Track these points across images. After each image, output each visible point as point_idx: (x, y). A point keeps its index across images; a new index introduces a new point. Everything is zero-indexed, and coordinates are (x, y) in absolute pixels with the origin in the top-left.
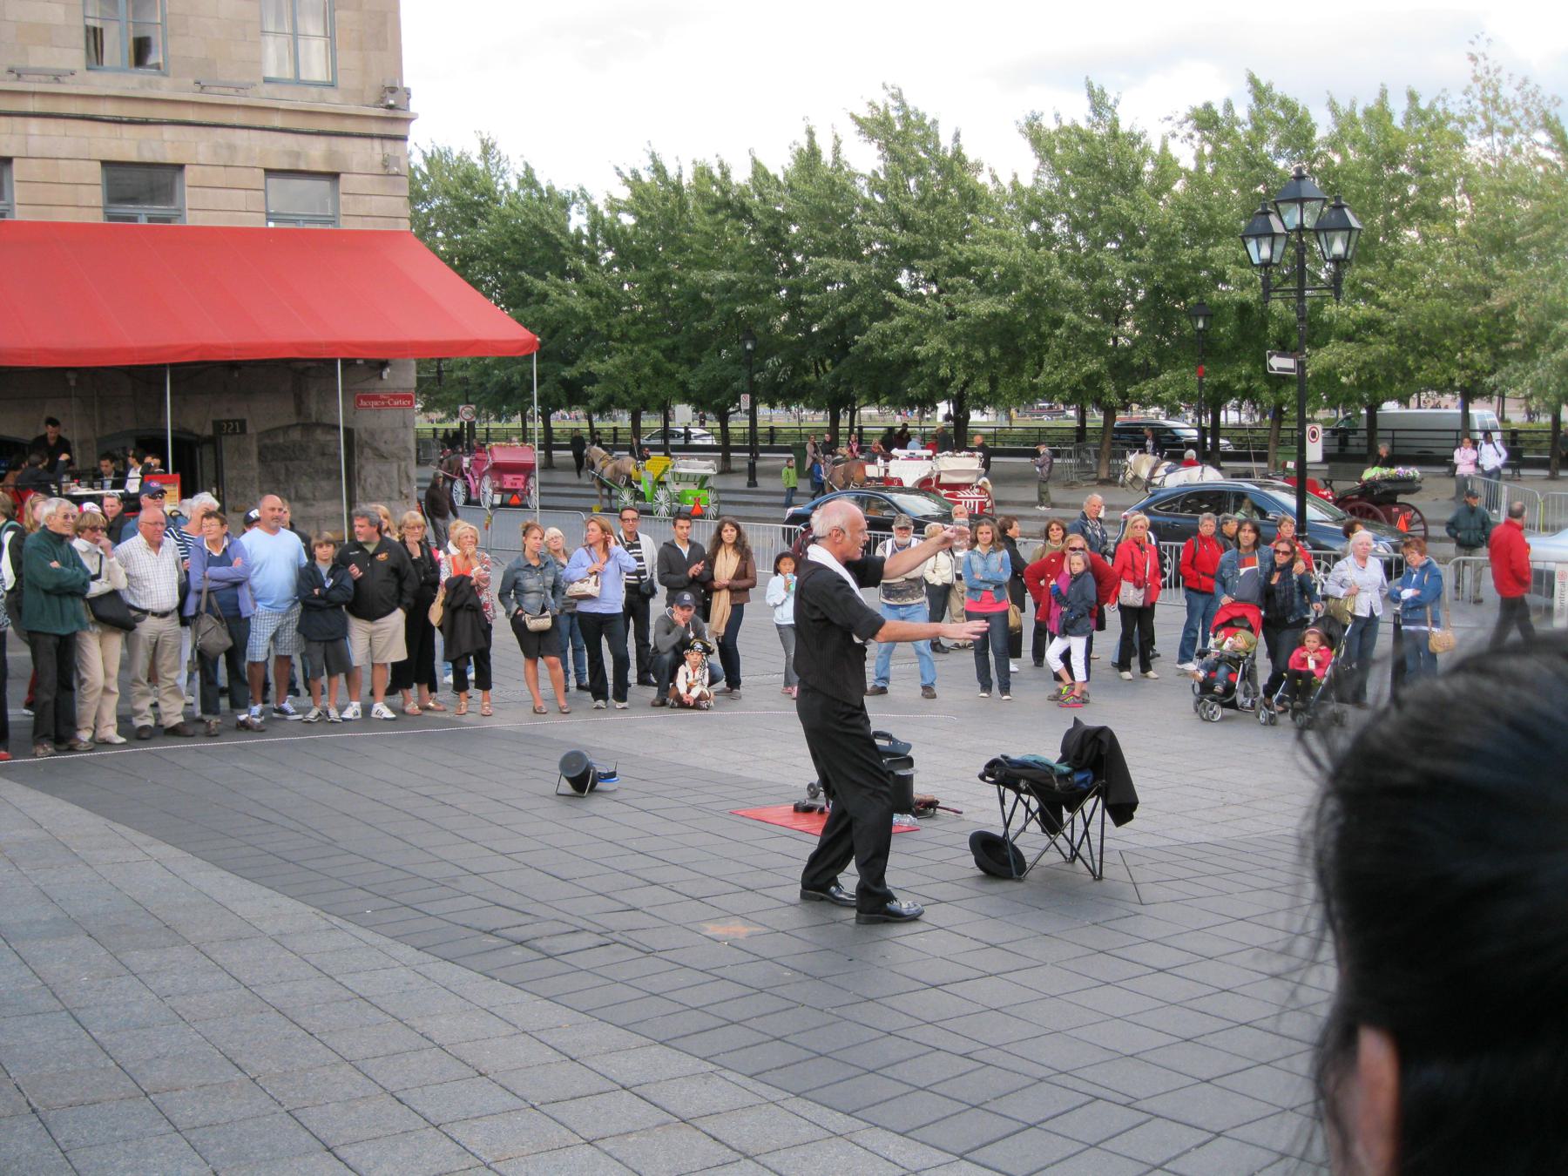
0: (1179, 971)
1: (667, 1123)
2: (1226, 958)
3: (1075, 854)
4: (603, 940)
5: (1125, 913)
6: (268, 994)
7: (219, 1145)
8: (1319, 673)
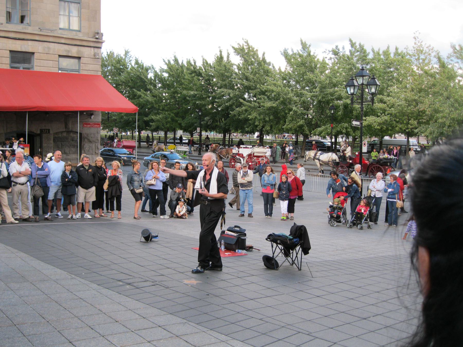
0: (323, 297)
3: (293, 263)
4: (153, 284)
7: (37, 340)
8: (365, 213)
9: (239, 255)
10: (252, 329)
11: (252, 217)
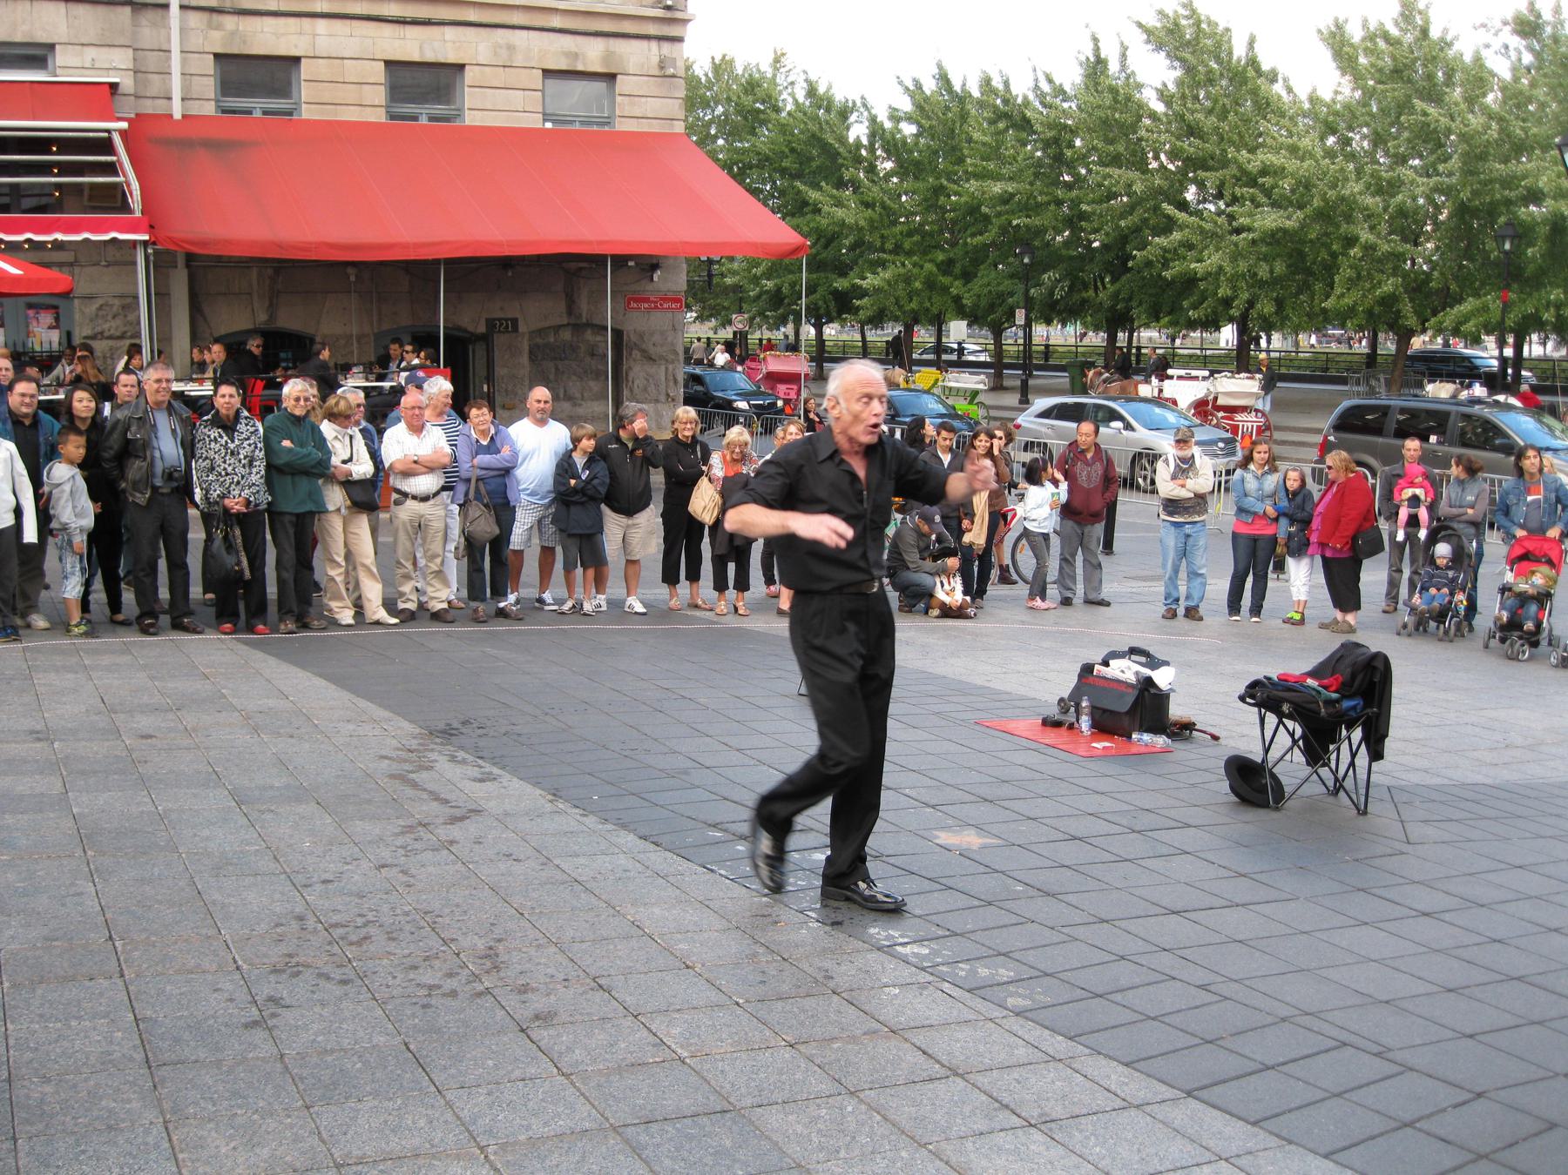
0: (1447, 917)
3: (1338, 787)
5: (1389, 851)
7: (414, 1015)
9: (1143, 750)
10: (1166, 1019)
11: (1201, 619)
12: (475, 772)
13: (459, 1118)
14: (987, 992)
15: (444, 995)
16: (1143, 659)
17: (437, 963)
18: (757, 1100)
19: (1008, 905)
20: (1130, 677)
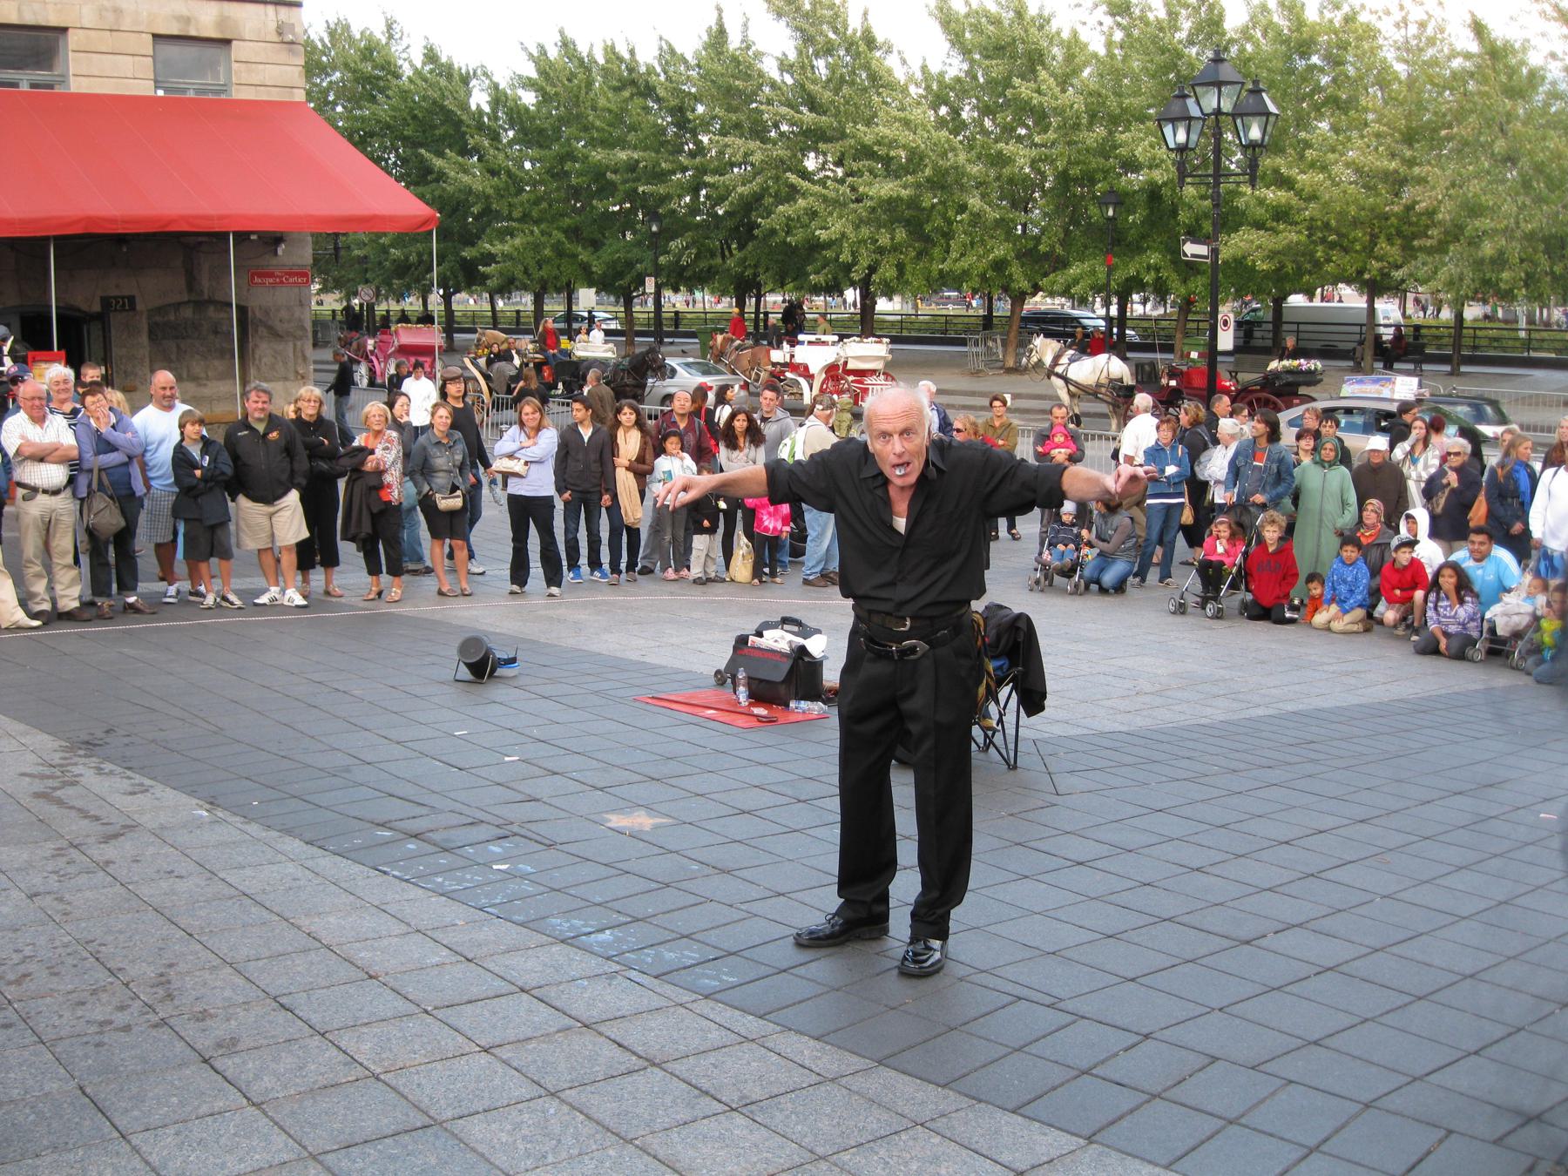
0: (1099, 864)
1: (569, 1029)
2: (1146, 851)
4: (500, 832)
5: (1040, 804)
6: (145, 891)
7: (86, 1056)
8: (1227, 561)
9: (800, 717)
12: (126, 785)
13: (147, 1163)
14: (675, 977)
15: (117, 1029)
16: (796, 629)
17: (104, 997)
18: (457, 1112)
19: (684, 885)
20: (783, 646)
